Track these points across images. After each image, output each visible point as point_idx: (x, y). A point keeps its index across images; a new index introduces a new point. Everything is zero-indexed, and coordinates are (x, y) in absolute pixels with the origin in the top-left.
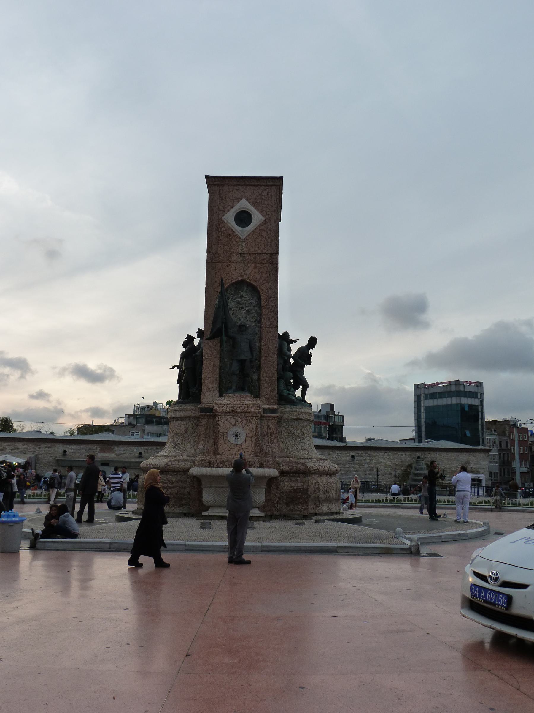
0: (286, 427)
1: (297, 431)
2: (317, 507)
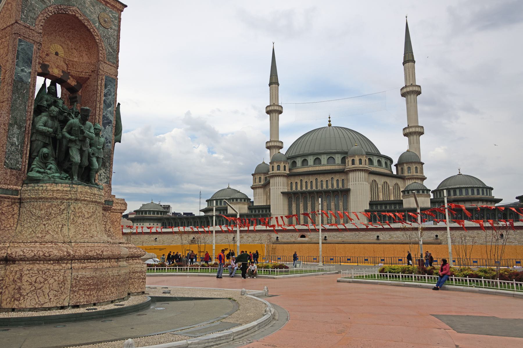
0: (27, 207)
1: (39, 212)
2: (16, 301)
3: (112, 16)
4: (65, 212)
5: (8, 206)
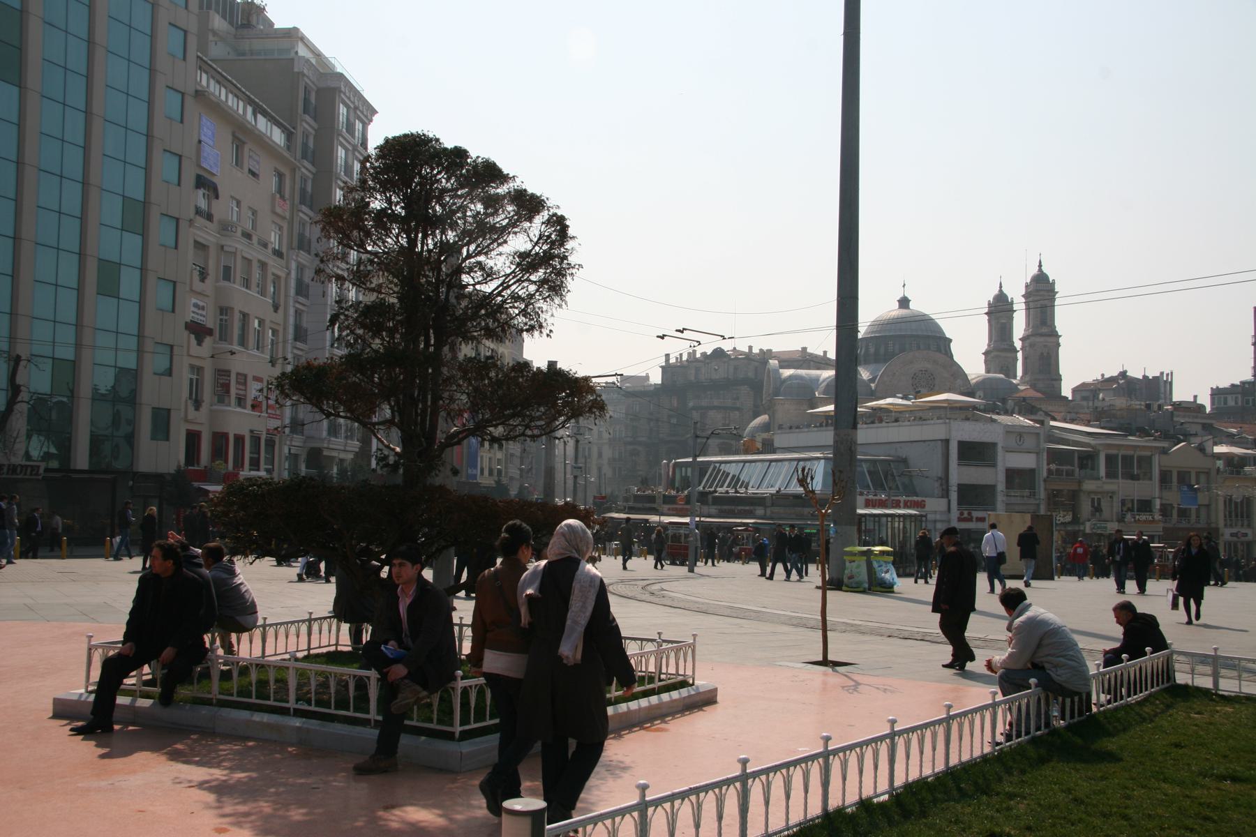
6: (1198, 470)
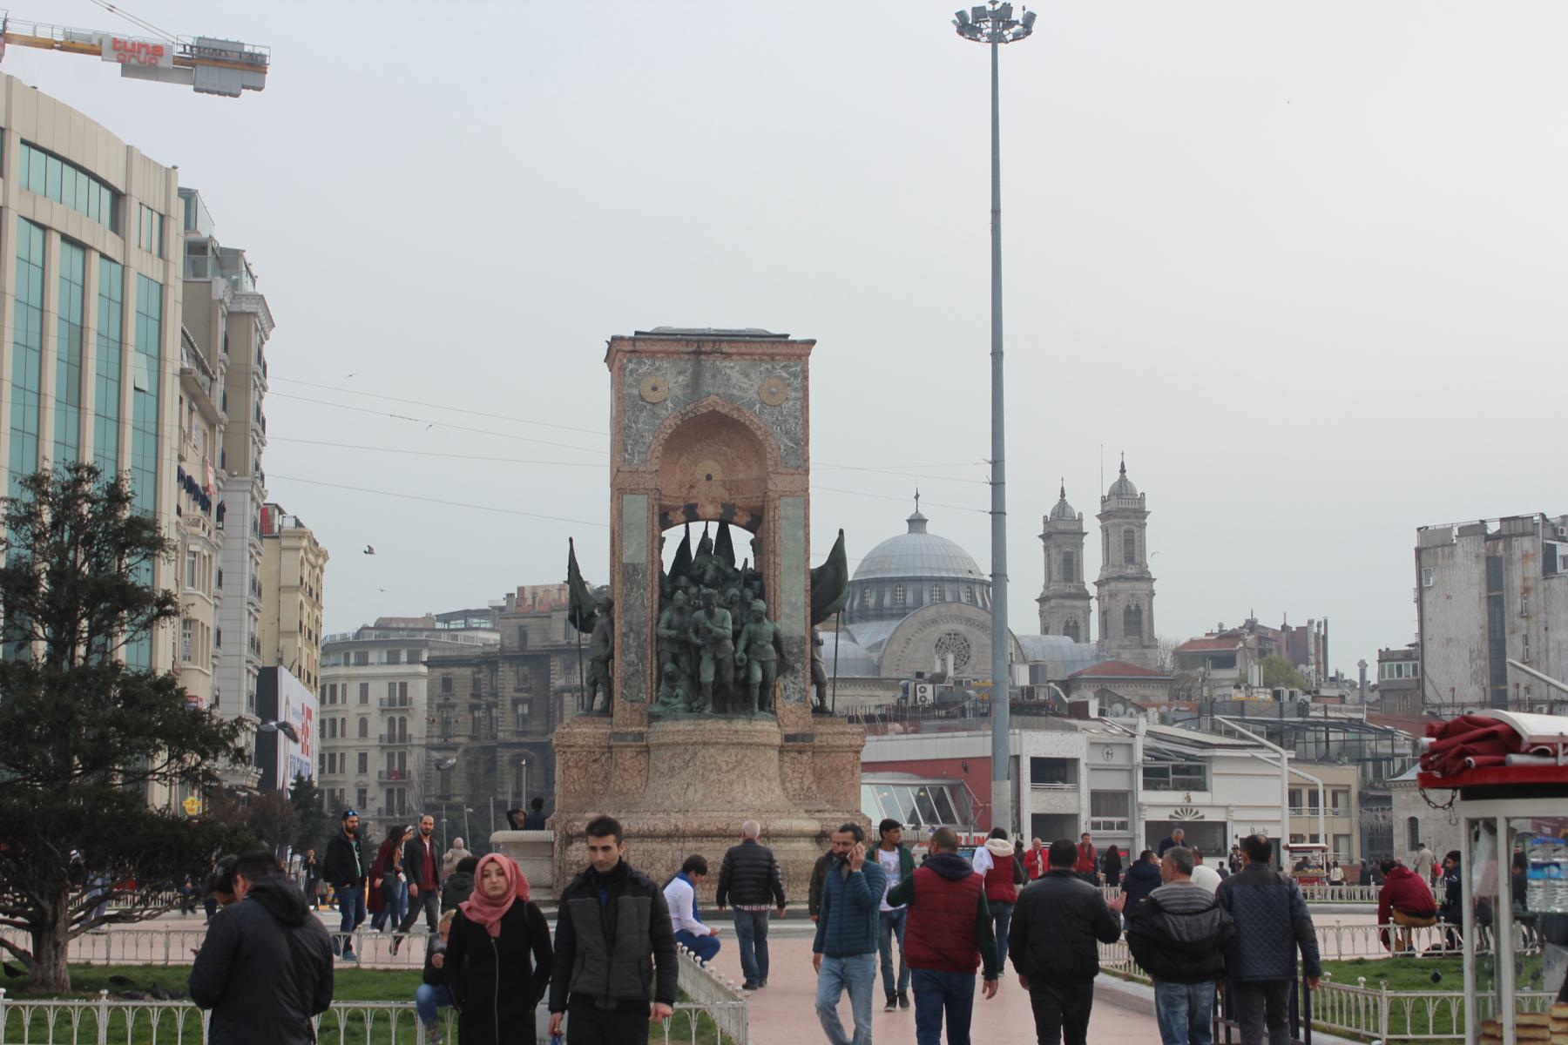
3: (789, 374)
4: (691, 764)
5: (632, 758)
6: (1335, 788)
